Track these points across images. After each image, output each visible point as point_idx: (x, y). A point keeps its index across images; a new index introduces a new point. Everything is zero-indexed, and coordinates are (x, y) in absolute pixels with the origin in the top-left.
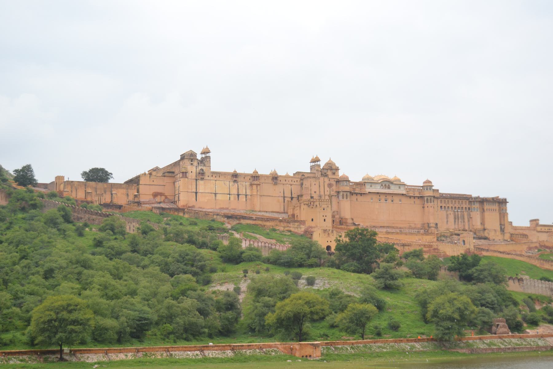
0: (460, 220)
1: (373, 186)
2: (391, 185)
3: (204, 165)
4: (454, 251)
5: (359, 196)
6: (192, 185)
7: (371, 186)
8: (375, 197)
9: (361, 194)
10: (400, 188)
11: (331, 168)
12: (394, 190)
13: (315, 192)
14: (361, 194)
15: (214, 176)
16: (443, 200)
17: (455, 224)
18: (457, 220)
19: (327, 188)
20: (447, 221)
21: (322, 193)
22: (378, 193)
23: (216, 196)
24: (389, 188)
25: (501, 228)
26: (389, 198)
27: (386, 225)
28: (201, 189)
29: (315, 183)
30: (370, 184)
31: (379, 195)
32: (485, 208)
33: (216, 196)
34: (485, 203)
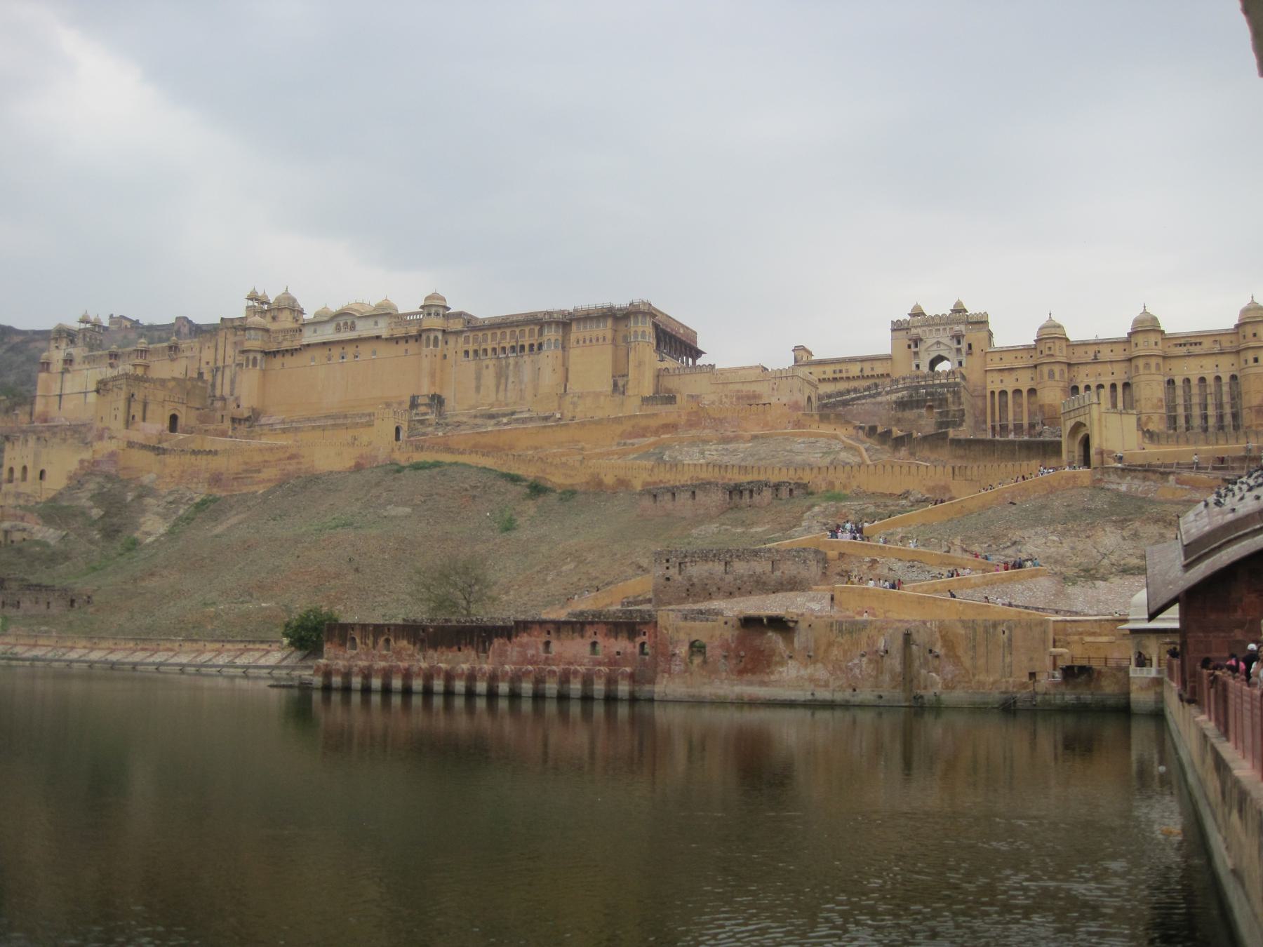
0: (511, 379)
1: (320, 329)
2: (357, 322)
5: (288, 358)
7: (315, 331)
8: (319, 354)
9: (292, 352)
11: (289, 306)
12: (365, 329)
14: (292, 352)
16: (471, 335)
17: (497, 391)
18: (503, 381)
19: (230, 351)
20: (478, 389)
21: (220, 364)
22: (324, 343)
24: (353, 328)
25: (615, 385)
26: (350, 350)
30: (312, 328)
32: (573, 337)
34: (574, 327)
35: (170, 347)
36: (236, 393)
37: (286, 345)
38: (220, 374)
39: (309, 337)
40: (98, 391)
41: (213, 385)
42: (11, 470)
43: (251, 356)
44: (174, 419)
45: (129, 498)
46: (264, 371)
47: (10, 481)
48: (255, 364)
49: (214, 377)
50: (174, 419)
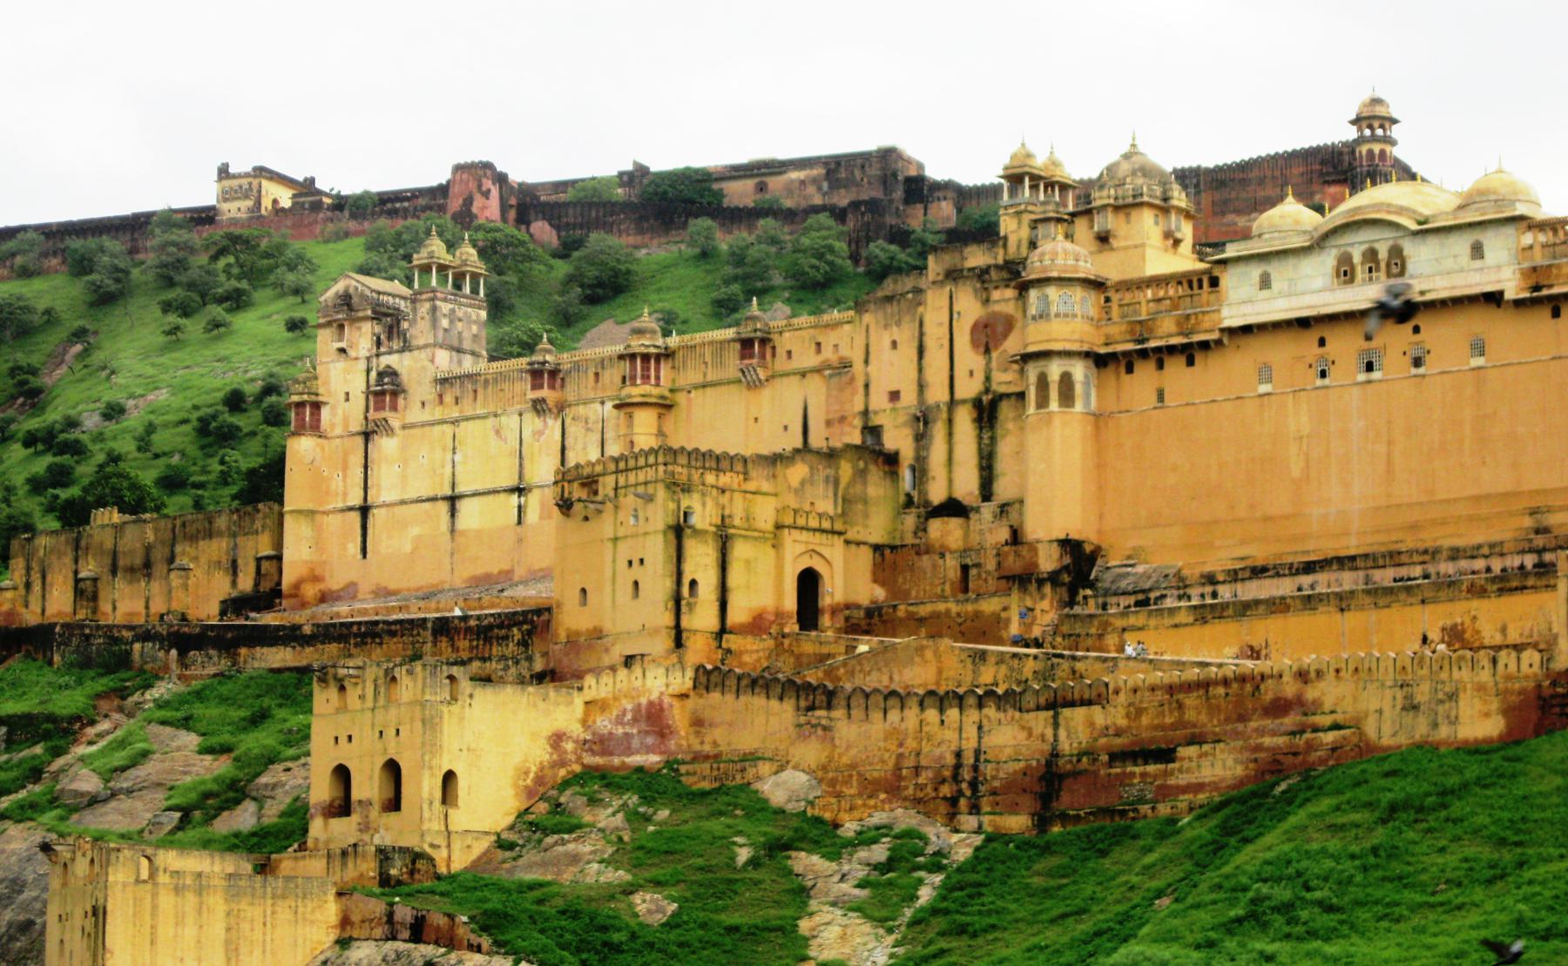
1: (1280, 273)
2: (1410, 248)
3: (406, 347)
4: (1412, 707)
5: (1175, 366)
6: (345, 468)
7: (1265, 283)
9: (1189, 353)
10: (1477, 251)
13: (895, 396)
15: (448, 398)
19: (969, 359)
22: (1303, 323)
23: (453, 512)
27: (1351, 546)
28: (386, 488)
29: (895, 333)
31: (1313, 336)
33: (453, 512)
35: (746, 344)
36: (1004, 488)
37: (1167, 332)
38: (938, 431)
39: (1242, 300)
40: (565, 506)
41: (920, 471)
42: (342, 774)
43: (1055, 370)
44: (809, 582)
45: (743, 855)
46: (1098, 419)
47: (342, 807)
48: (1067, 397)
49: (921, 438)
50: (809, 582)
